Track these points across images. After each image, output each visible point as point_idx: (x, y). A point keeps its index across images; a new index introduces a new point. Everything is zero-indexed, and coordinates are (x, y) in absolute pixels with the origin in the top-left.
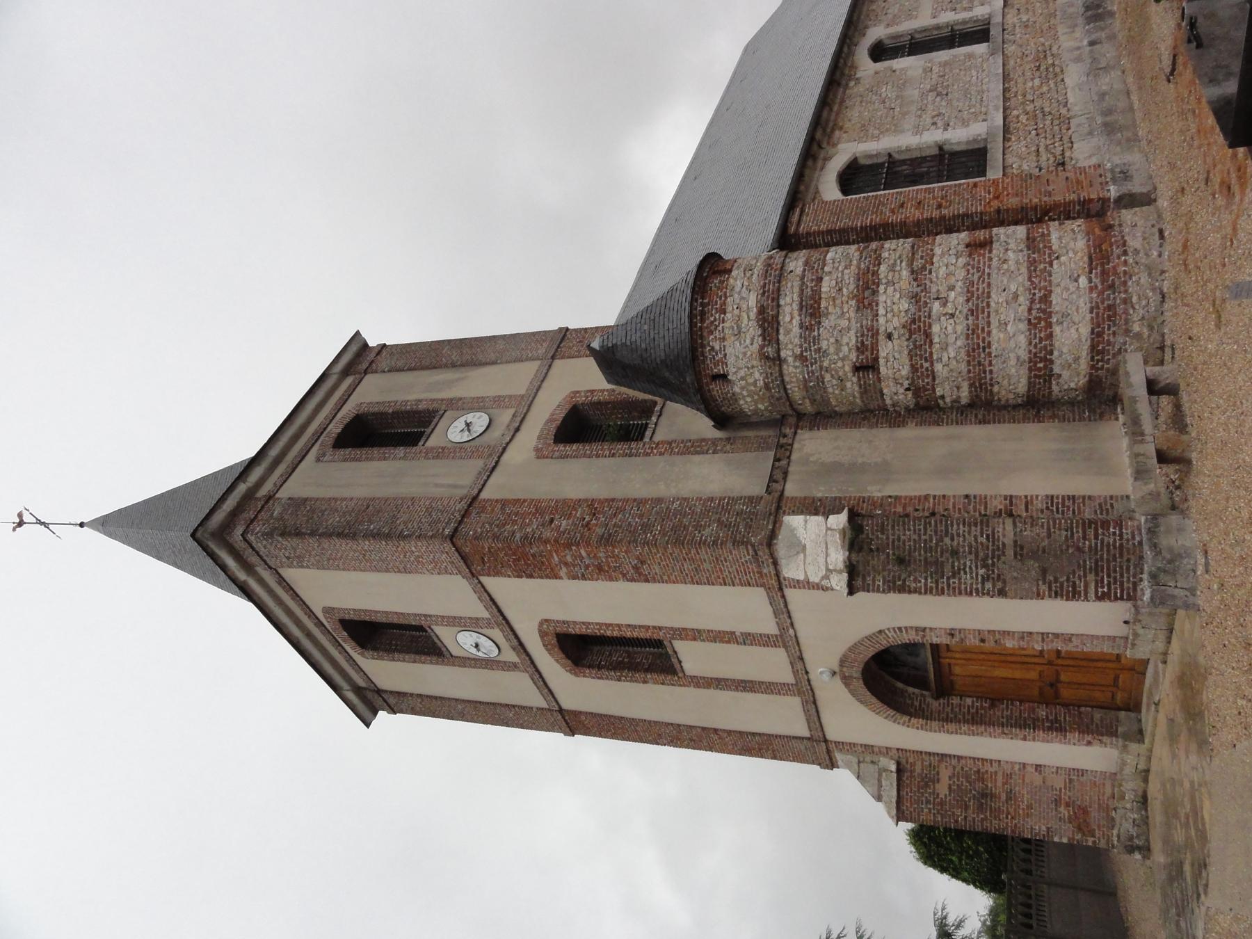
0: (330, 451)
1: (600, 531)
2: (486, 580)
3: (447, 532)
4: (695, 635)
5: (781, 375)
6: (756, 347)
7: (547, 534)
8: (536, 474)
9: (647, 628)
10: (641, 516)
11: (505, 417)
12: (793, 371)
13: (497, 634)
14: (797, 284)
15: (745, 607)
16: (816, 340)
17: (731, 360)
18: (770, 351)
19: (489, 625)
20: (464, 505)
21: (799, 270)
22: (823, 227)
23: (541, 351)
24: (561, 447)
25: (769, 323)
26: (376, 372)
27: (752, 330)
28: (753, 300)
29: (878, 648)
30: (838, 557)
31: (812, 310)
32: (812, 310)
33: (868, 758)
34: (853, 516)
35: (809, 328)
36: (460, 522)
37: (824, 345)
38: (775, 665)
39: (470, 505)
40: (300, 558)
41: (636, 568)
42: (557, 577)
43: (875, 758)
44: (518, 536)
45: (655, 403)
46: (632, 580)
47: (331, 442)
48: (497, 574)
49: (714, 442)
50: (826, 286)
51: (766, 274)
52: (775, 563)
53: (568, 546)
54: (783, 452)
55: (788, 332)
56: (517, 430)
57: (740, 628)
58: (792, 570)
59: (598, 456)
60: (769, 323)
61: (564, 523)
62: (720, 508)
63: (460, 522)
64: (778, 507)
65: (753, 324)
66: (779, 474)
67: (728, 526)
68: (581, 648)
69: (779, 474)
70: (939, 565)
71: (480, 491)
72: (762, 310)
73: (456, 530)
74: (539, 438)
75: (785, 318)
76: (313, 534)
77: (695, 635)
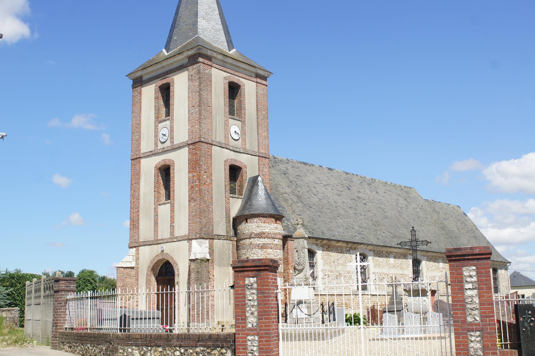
0: (227, 81)
1: (203, 189)
2: (186, 149)
3: (202, 139)
4: (172, 211)
5: (246, 238)
6: (254, 231)
7: (202, 172)
8: (220, 160)
9: (174, 196)
10: (208, 200)
11: (239, 144)
12: (247, 241)
13: (168, 144)
14: (271, 242)
15: (182, 228)
16: (255, 248)
17: (251, 224)
18: (253, 236)
19: (172, 142)
20: (210, 142)
21: (275, 243)
22: (289, 247)
23: (261, 151)
24: (228, 168)
25: (260, 235)
26: (257, 86)
27: (259, 230)
28: (267, 230)
29: (172, 264)
30: (199, 256)
31: (263, 247)
32: (263, 247)
33: (134, 258)
34: (208, 260)
35: (258, 246)
36: (205, 143)
37: (254, 250)
38: (164, 232)
39: (210, 144)
40: (192, 80)
41: (193, 198)
42: (189, 172)
43: (135, 260)
44: (201, 163)
45: (241, 195)
46: (189, 197)
47: (231, 80)
48: (189, 153)
49: (229, 217)
50: (270, 250)
51: (274, 234)
52: (196, 239)
53: (199, 179)
54: (227, 238)
55: (258, 240)
56: (234, 151)
57: (176, 224)
58: (194, 242)
59: (225, 181)
60: (260, 235)
61: (205, 177)
62: (210, 221)
63: (205, 143)
64: (211, 239)
65: (261, 231)
66: (219, 237)
67: (205, 225)
68: (165, 172)
69: (219, 237)
70: (198, 280)
71: (214, 145)
72: (264, 233)
73: (202, 142)
74: (231, 159)
75: (261, 240)
76: (200, 89)
77: (172, 211)
